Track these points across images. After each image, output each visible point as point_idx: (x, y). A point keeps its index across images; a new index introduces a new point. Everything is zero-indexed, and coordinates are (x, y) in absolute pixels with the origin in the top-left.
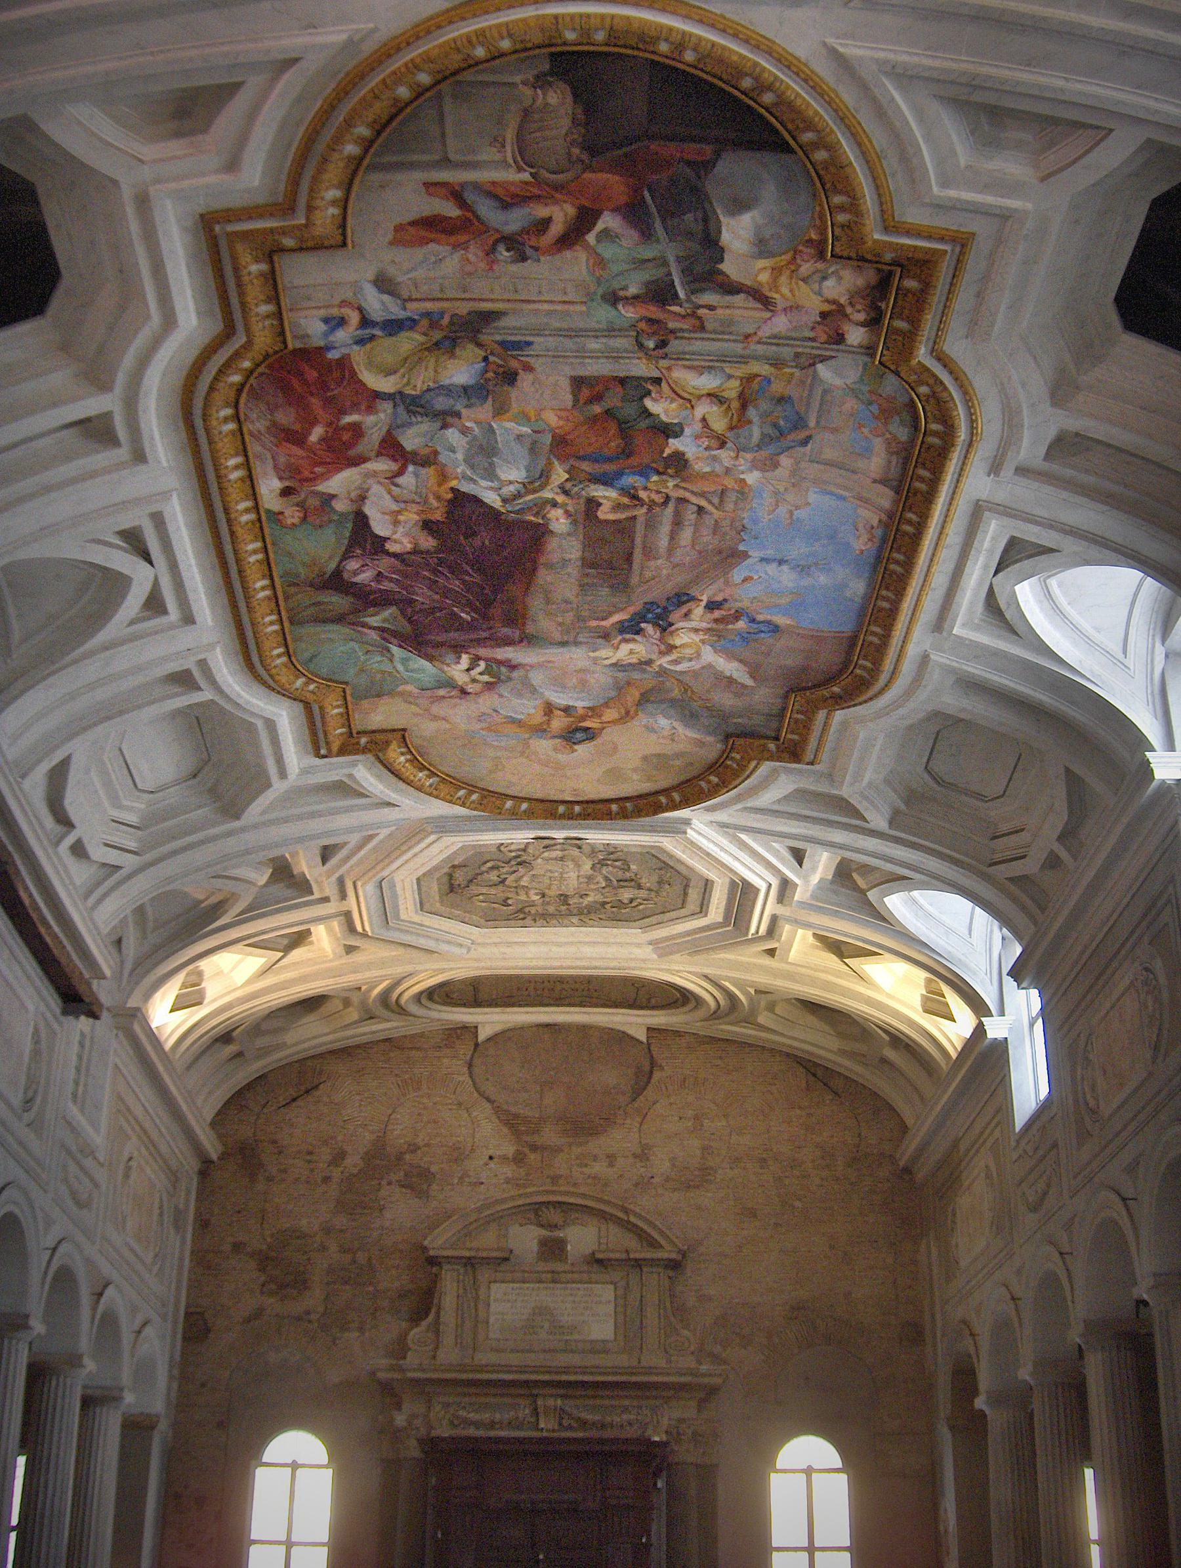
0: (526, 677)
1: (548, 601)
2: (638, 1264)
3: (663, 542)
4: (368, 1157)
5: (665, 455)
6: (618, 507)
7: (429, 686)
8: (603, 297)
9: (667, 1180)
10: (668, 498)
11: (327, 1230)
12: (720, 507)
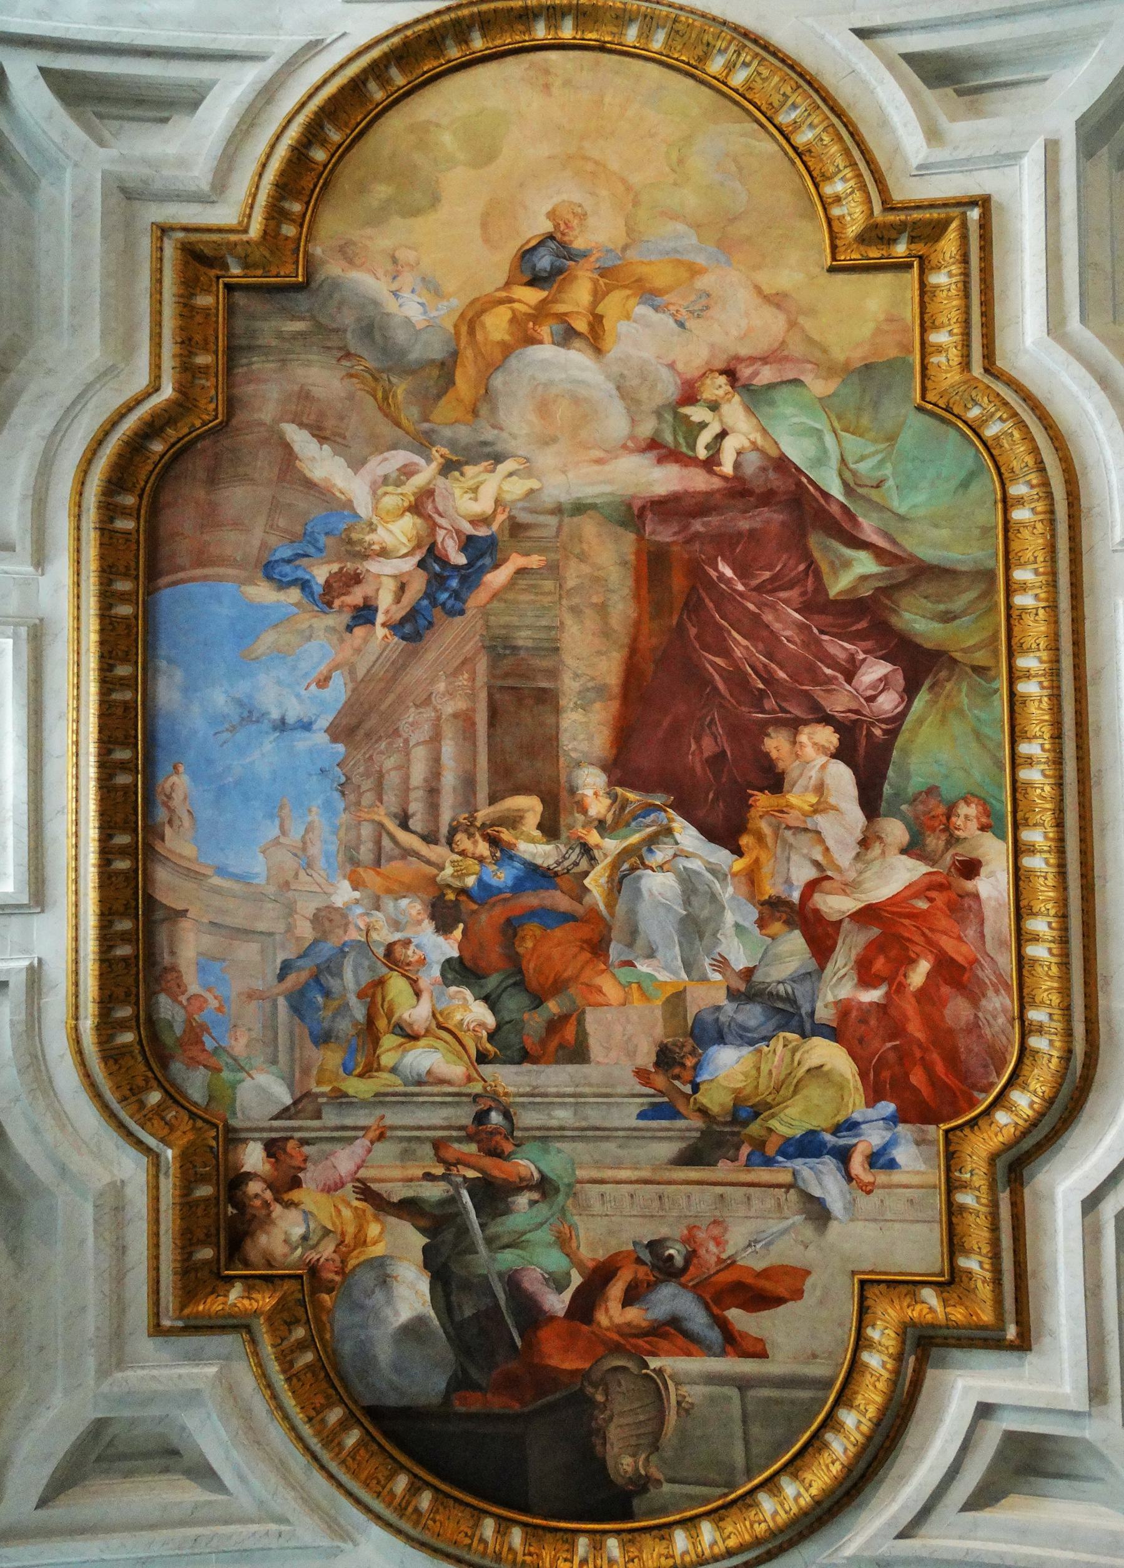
0: (633, 422)
1: (602, 609)
3: (448, 750)
5: (461, 926)
6: (513, 821)
7: (785, 390)
8: (557, 1190)
10: (450, 842)
12: (381, 825)
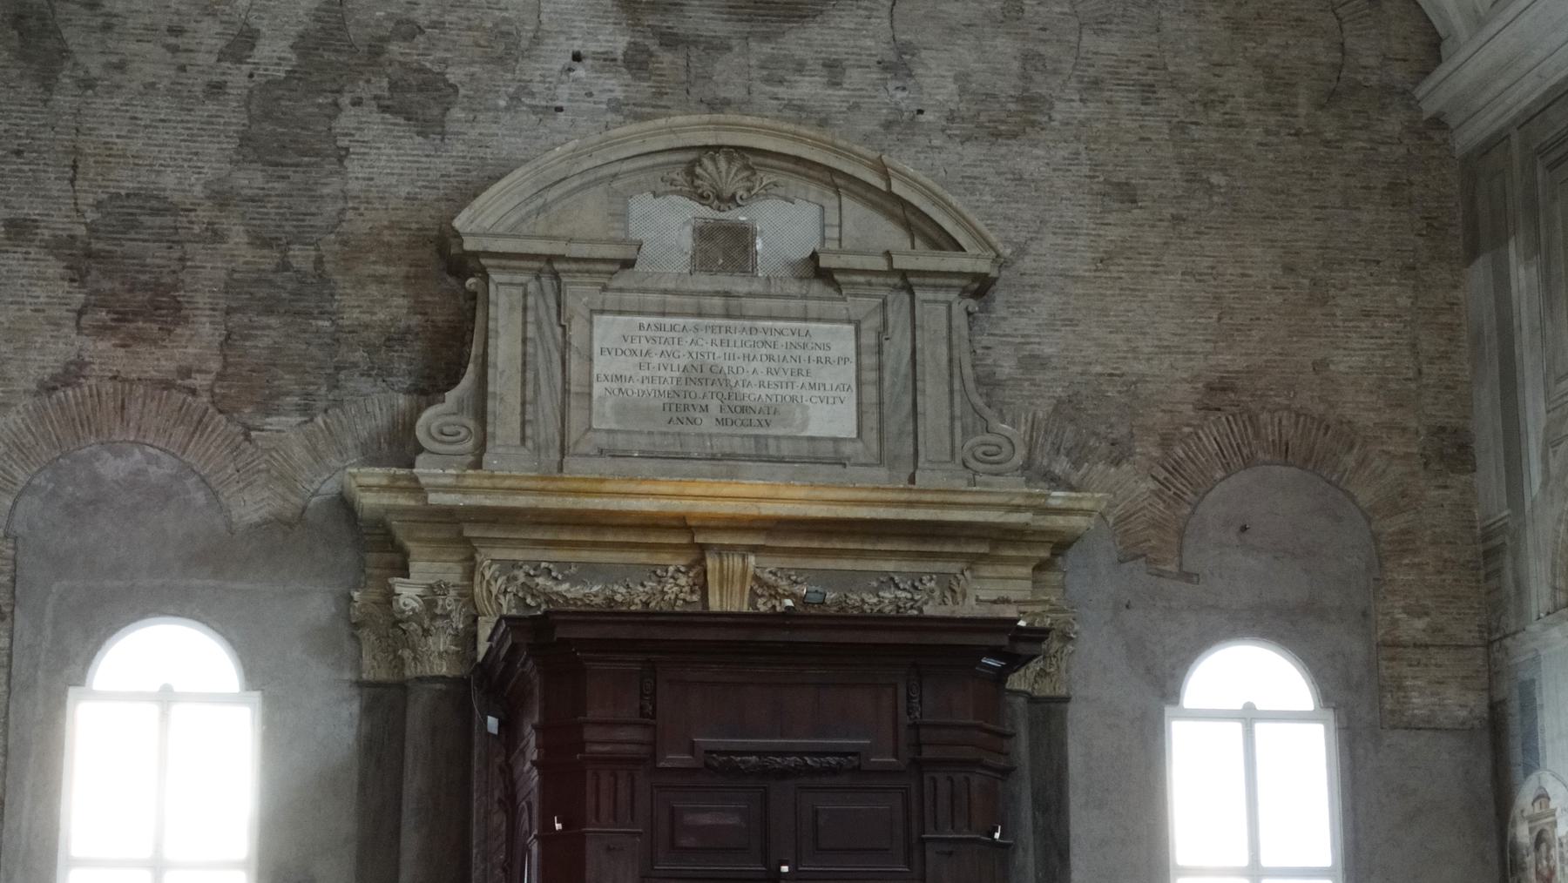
2: (906, 281)
4: (305, 46)
9: (951, 117)
11: (222, 198)
